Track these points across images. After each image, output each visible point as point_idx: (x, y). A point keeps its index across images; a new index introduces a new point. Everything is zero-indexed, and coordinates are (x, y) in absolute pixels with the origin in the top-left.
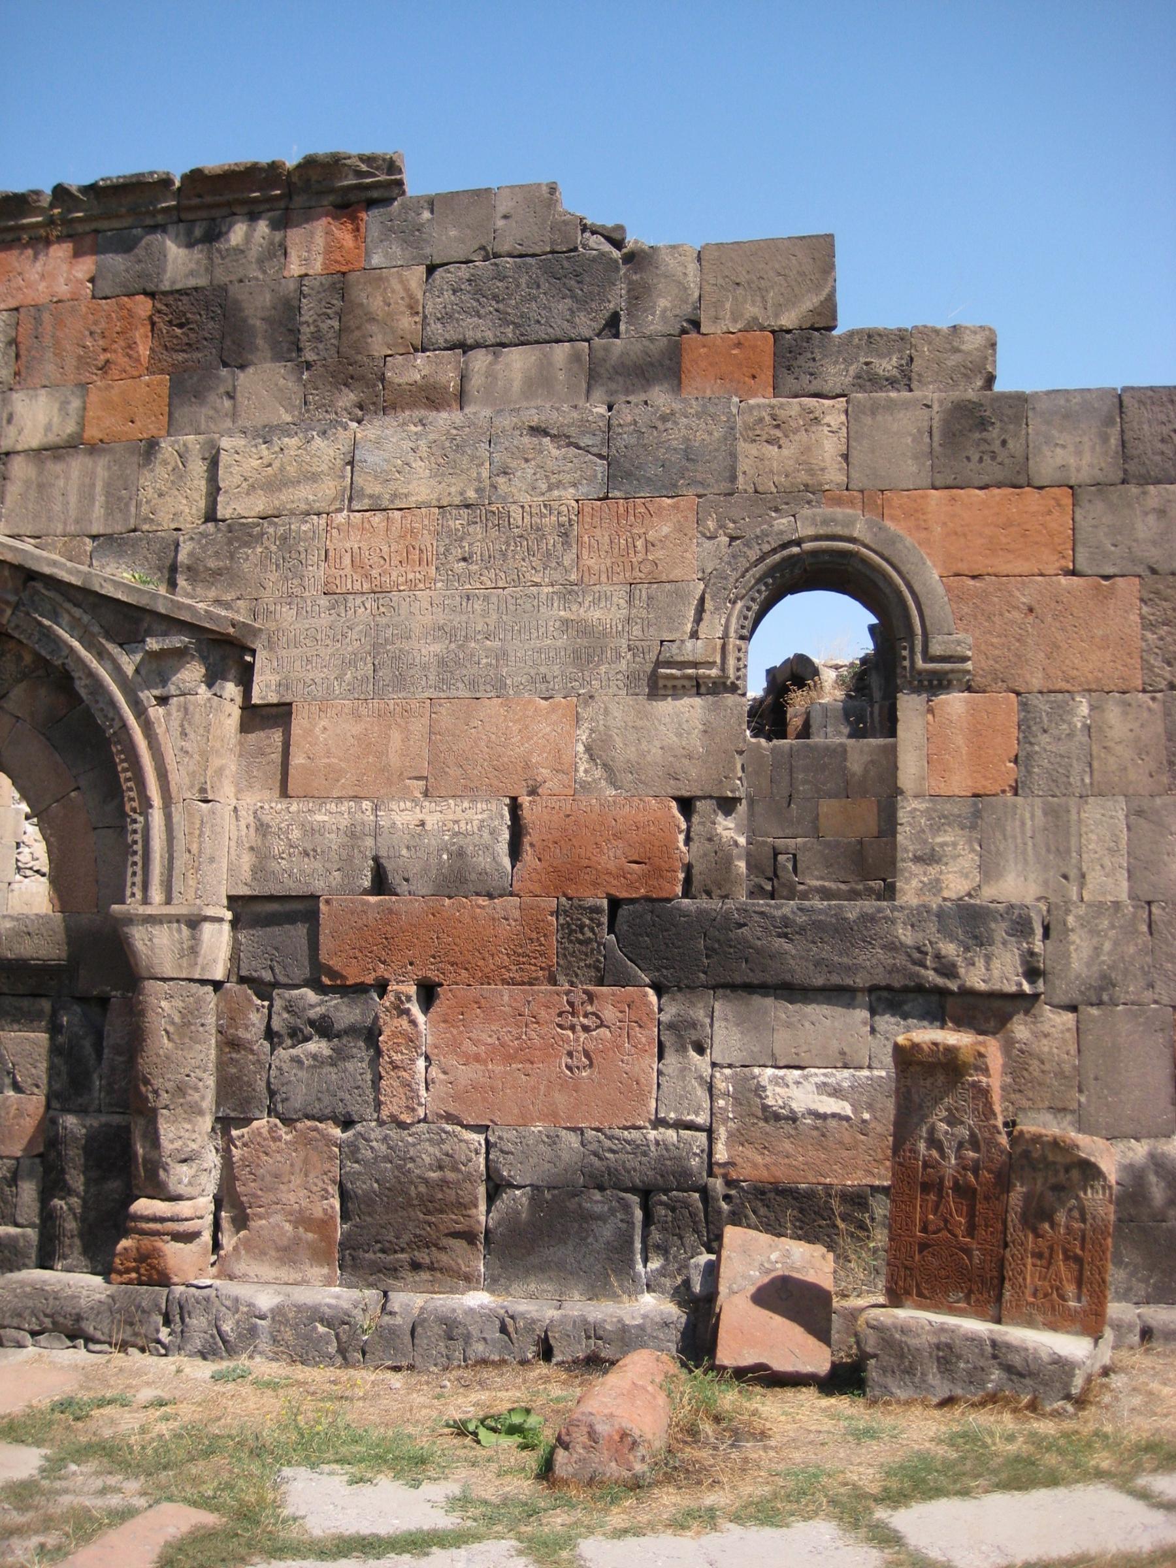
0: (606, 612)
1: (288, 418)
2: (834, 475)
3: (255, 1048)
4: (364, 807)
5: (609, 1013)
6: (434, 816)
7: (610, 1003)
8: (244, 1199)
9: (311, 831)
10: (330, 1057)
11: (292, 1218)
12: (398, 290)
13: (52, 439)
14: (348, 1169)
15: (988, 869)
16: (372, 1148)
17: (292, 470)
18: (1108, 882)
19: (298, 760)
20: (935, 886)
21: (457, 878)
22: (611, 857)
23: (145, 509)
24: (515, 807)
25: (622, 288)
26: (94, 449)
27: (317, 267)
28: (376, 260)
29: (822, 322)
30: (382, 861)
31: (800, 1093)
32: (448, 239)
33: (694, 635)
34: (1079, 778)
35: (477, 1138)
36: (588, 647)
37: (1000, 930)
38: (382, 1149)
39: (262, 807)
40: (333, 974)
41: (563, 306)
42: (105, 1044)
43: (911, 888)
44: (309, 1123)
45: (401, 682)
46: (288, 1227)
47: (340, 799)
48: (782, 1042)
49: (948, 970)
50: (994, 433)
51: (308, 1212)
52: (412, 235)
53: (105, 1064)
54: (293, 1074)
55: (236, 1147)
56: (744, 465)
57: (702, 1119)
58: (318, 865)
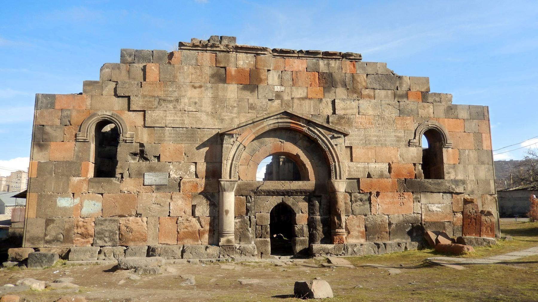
0: (401, 134)
1: (345, 97)
2: (432, 115)
5: (406, 197)
6: (377, 165)
7: (406, 195)
9: (357, 167)
12: (362, 78)
13: (302, 96)
15: (456, 175)
17: (349, 107)
18: (472, 177)
19: (354, 155)
20: (450, 177)
21: (381, 176)
22: (405, 172)
23: (321, 111)
24: (389, 164)
25: (398, 82)
26: (310, 99)
27: (348, 72)
28: (358, 72)
29: (428, 91)
31: (434, 208)
32: (370, 70)
33: (415, 138)
34: (467, 162)
35: (387, 217)
36: (399, 139)
37: (460, 184)
38: (372, 219)
40: (362, 191)
41: (389, 84)
43: (446, 177)
45: (370, 144)
48: (431, 201)
49: (454, 189)
50: (453, 111)
52: (364, 69)
54: (356, 207)
56: (420, 113)
57: (420, 212)
58: (359, 173)
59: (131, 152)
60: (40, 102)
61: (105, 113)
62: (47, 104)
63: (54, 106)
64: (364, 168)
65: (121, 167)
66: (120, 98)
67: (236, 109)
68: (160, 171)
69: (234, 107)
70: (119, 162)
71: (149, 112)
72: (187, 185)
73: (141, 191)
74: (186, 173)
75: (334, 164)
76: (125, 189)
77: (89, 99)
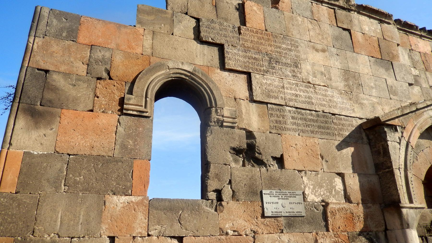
59: (233, 146)
60: (43, 23)
61: (181, 66)
62: (62, 30)
63: (76, 37)
65: (217, 176)
66: (206, 47)
67: (374, 90)
68: (287, 186)
69: (372, 88)
70: (212, 166)
71: (258, 76)
72: (338, 216)
73: (260, 231)
74: (331, 192)
76: (228, 226)
77: (150, 37)
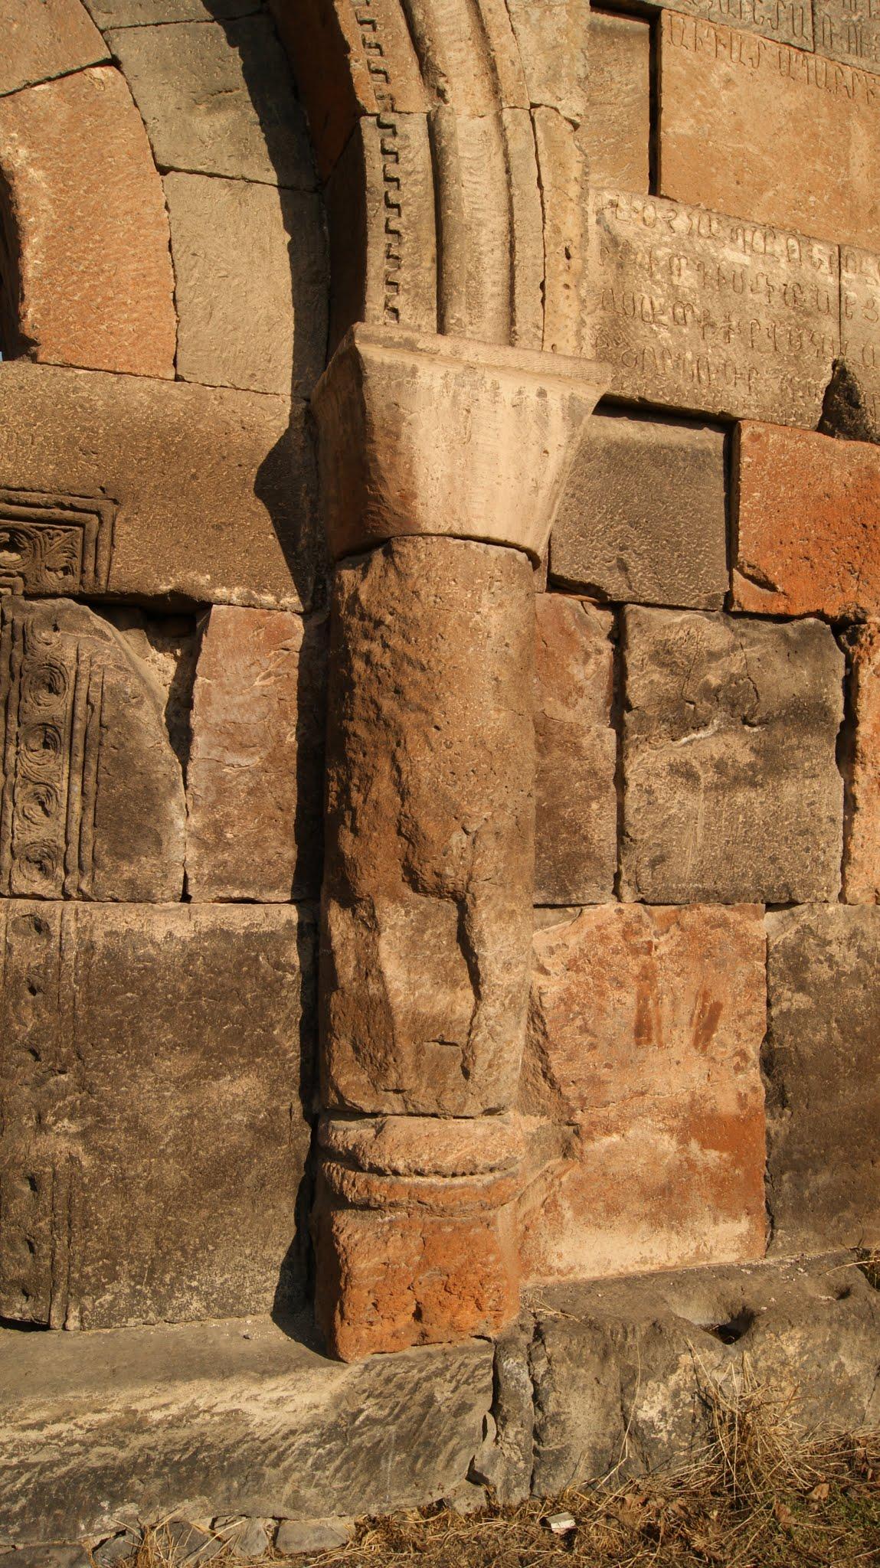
3: (586, 742)
4: (816, 255)
8: (570, 1092)
10: (752, 766)
11: (675, 1123)
14: (785, 1005)
16: (830, 959)
19: (676, 126)
30: (853, 369)
39: (614, 205)
42: (195, 720)
44: (707, 910)
46: (668, 1144)
47: (771, 231)
51: (709, 1105)
53: (197, 773)
55: (543, 970)
64: (792, 295)
75: (414, 98)
